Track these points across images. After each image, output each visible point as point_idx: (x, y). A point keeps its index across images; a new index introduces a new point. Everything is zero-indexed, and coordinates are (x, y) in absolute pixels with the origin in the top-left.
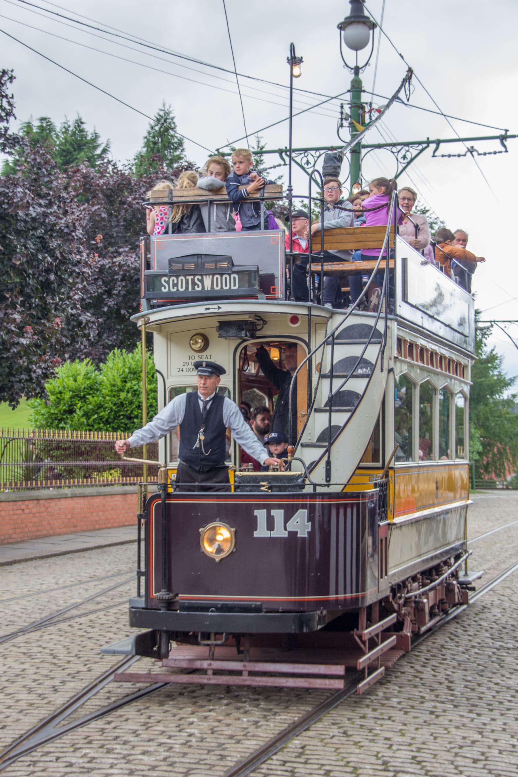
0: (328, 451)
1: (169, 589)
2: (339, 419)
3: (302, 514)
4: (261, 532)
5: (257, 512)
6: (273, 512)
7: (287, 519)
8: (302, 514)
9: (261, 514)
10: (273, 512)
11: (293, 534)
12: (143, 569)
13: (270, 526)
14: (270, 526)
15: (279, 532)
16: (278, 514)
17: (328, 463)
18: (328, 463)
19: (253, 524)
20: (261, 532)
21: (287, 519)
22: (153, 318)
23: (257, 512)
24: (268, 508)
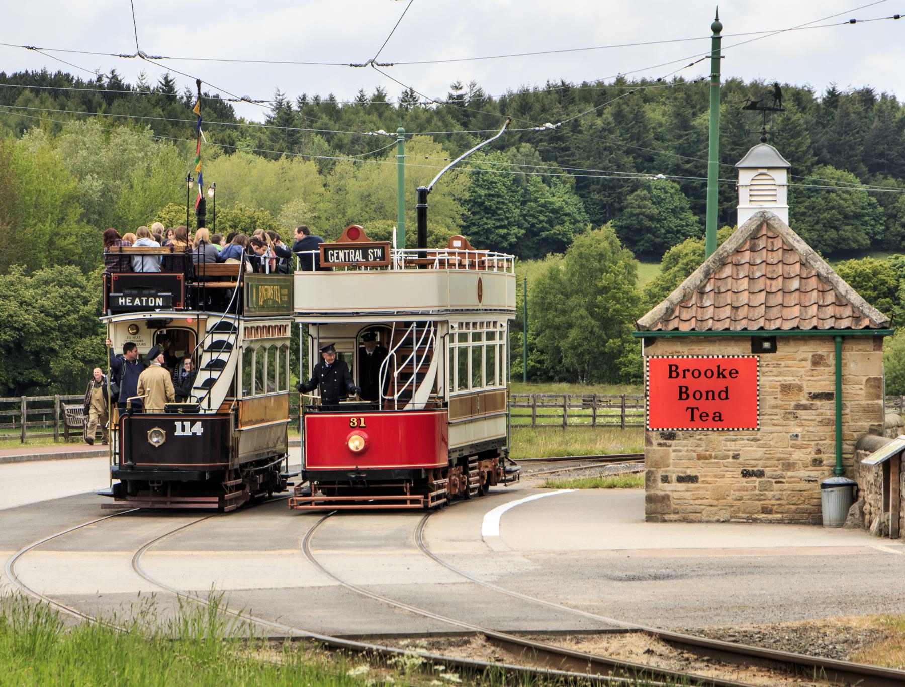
0: (209, 392)
1: (131, 460)
2: (215, 375)
3: (199, 424)
4: (178, 432)
5: (176, 423)
6: (185, 423)
7: (191, 426)
8: (199, 424)
9: (178, 424)
10: (185, 423)
11: (194, 434)
12: (117, 451)
13: (183, 429)
14: (183, 429)
15: (188, 433)
16: (187, 424)
17: (209, 398)
18: (209, 398)
19: (174, 428)
20: (178, 432)
21: (191, 426)
22: (114, 320)
23: (176, 423)
24: (182, 421)
